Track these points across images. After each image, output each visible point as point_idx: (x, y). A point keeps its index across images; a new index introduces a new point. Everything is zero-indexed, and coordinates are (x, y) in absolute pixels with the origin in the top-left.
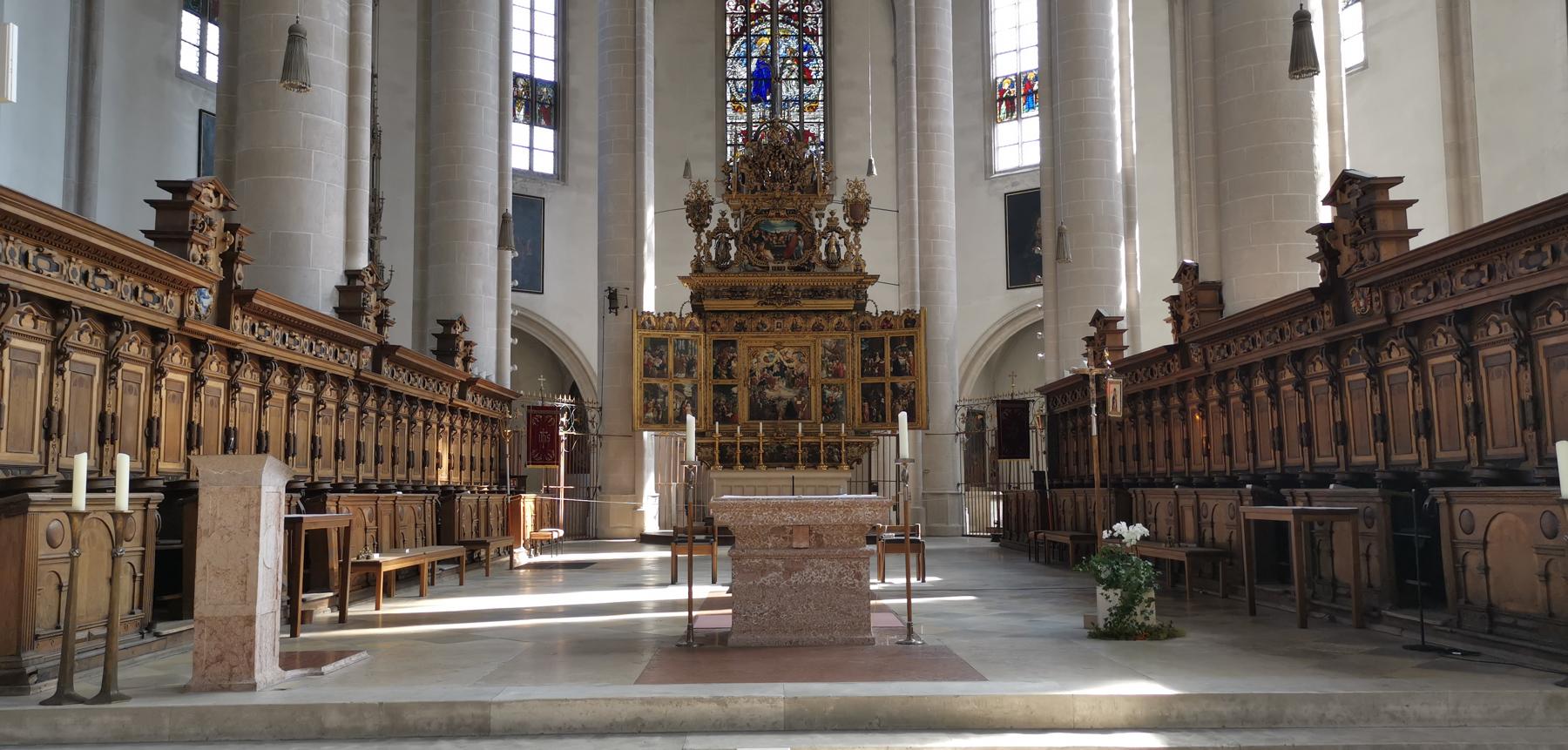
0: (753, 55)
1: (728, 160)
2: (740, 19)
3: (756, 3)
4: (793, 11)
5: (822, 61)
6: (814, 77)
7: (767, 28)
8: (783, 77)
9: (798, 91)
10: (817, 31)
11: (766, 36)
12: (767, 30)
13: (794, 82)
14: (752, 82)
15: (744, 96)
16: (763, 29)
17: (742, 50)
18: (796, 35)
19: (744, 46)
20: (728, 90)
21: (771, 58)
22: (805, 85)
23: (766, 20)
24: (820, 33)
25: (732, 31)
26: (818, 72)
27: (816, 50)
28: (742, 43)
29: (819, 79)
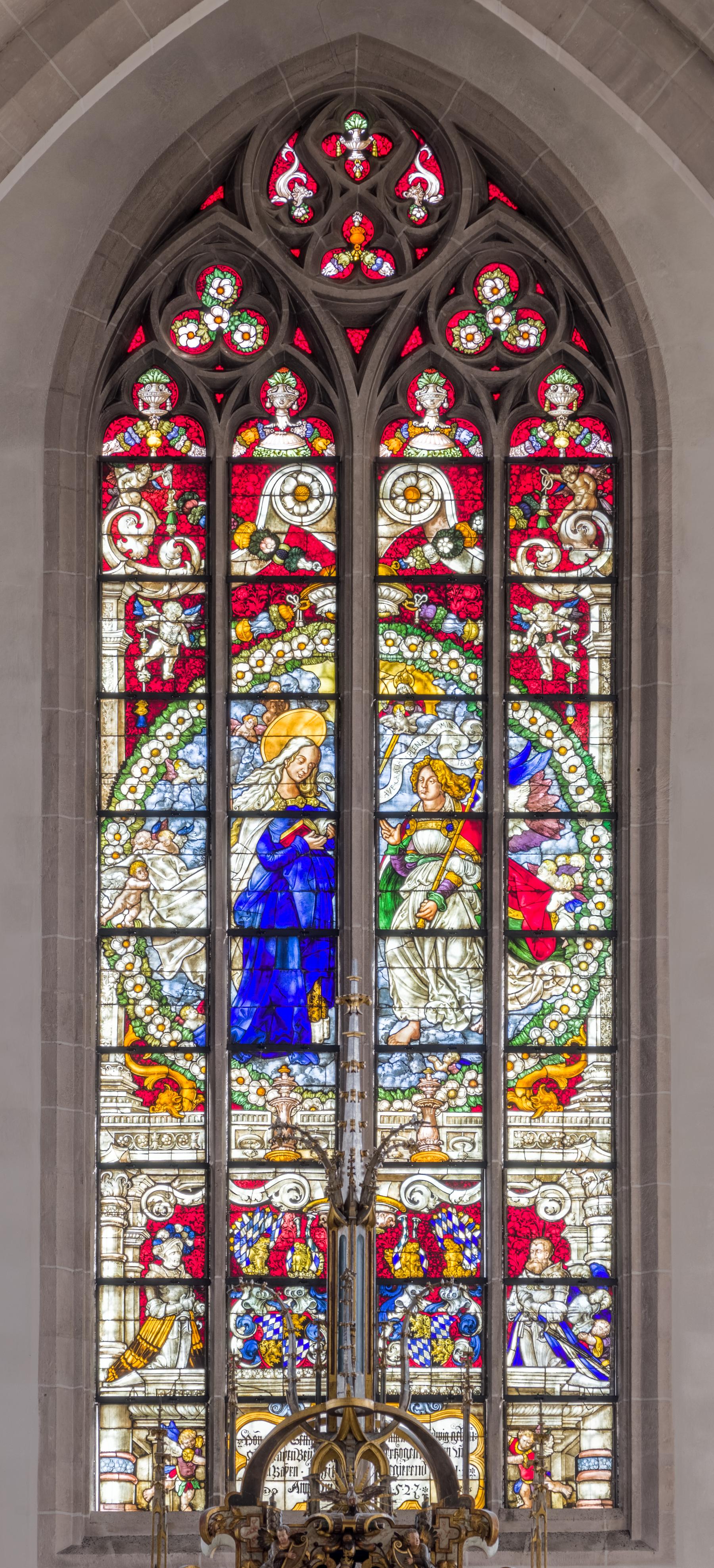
0: (243, 800)
1: (105, 1362)
2: (172, 609)
3: (261, 522)
4: (456, 566)
5: (606, 838)
6: (564, 923)
7: (317, 657)
8: (402, 920)
9: (477, 996)
10: (583, 676)
11: (305, 698)
12: (317, 669)
13: (456, 949)
14: (237, 949)
15: (193, 1020)
16: (297, 664)
17: (184, 774)
18: (468, 698)
19: (196, 753)
20: (108, 992)
21: (338, 816)
22: (514, 966)
23: (311, 615)
24: (594, 688)
25: (130, 673)
26: (581, 895)
27: (576, 779)
28: (189, 738)
29: (590, 935)
